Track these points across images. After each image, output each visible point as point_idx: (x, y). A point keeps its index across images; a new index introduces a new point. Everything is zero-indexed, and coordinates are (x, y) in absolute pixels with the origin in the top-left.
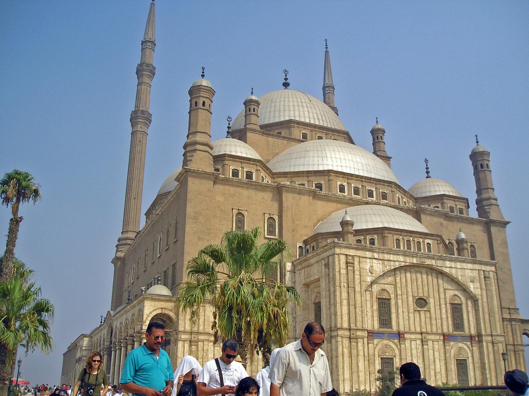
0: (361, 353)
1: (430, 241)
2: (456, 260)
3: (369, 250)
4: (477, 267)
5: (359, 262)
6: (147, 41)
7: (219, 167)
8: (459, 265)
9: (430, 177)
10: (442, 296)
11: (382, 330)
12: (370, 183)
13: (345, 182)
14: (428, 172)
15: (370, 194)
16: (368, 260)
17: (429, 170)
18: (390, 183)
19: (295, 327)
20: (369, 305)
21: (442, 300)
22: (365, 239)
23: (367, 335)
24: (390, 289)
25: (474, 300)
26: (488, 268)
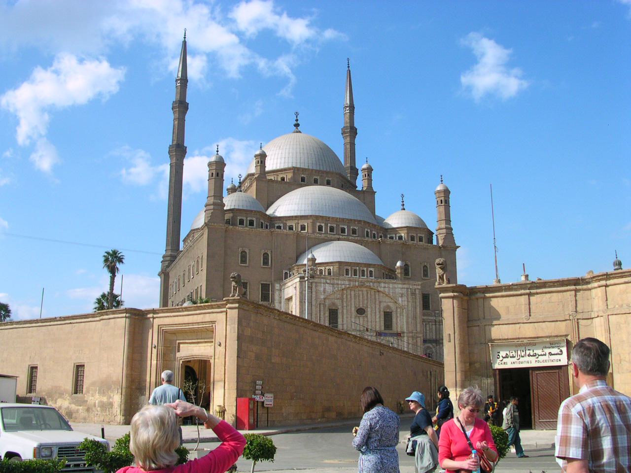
1: (372, 269)
2: (388, 283)
3: (323, 278)
4: (405, 286)
5: (316, 286)
8: (391, 286)
9: (404, 209)
10: (378, 306)
13: (323, 223)
15: (343, 231)
16: (322, 285)
18: (360, 221)
21: (377, 309)
24: (338, 302)
25: (402, 308)
26: (415, 287)
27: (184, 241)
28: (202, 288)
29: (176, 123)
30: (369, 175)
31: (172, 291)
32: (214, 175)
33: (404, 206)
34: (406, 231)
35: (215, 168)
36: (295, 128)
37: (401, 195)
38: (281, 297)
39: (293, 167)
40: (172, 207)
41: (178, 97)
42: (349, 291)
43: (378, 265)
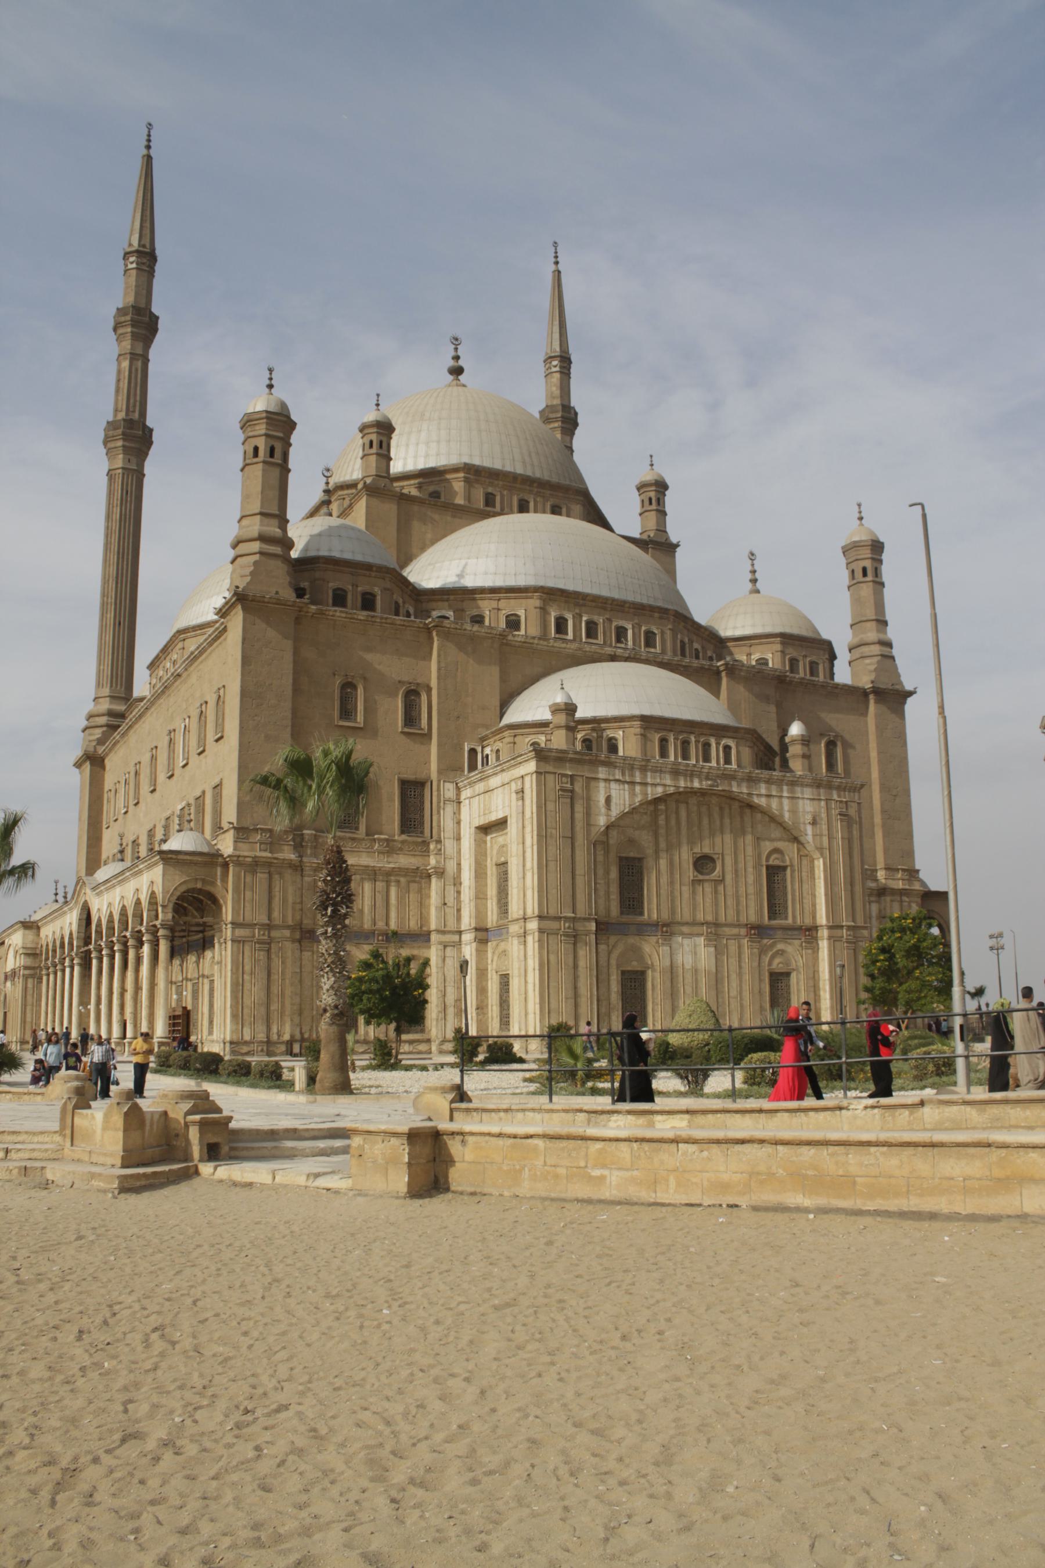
0: (582, 963)
1: (731, 743)
6: (137, 251)
7: (305, 584)
9: (758, 592)
10: (750, 850)
11: (625, 919)
12: (623, 612)
13: (569, 610)
14: (754, 581)
16: (602, 784)
17: (757, 575)
19: (459, 910)
20: (600, 872)
22: (602, 737)
23: (594, 928)
24: (645, 838)
27: (153, 666)
28: (225, 792)
29: (126, 364)
30: (660, 501)
31: (114, 805)
32: (261, 452)
33: (758, 584)
34: (778, 647)
35: (263, 432)
36: (451, 377)
37: (747, 553)
38: (459, 823)
39: (465, 464)
40: (112, 584)
41: (131, 299)
42: (672, 805)
43: (748, 731)
